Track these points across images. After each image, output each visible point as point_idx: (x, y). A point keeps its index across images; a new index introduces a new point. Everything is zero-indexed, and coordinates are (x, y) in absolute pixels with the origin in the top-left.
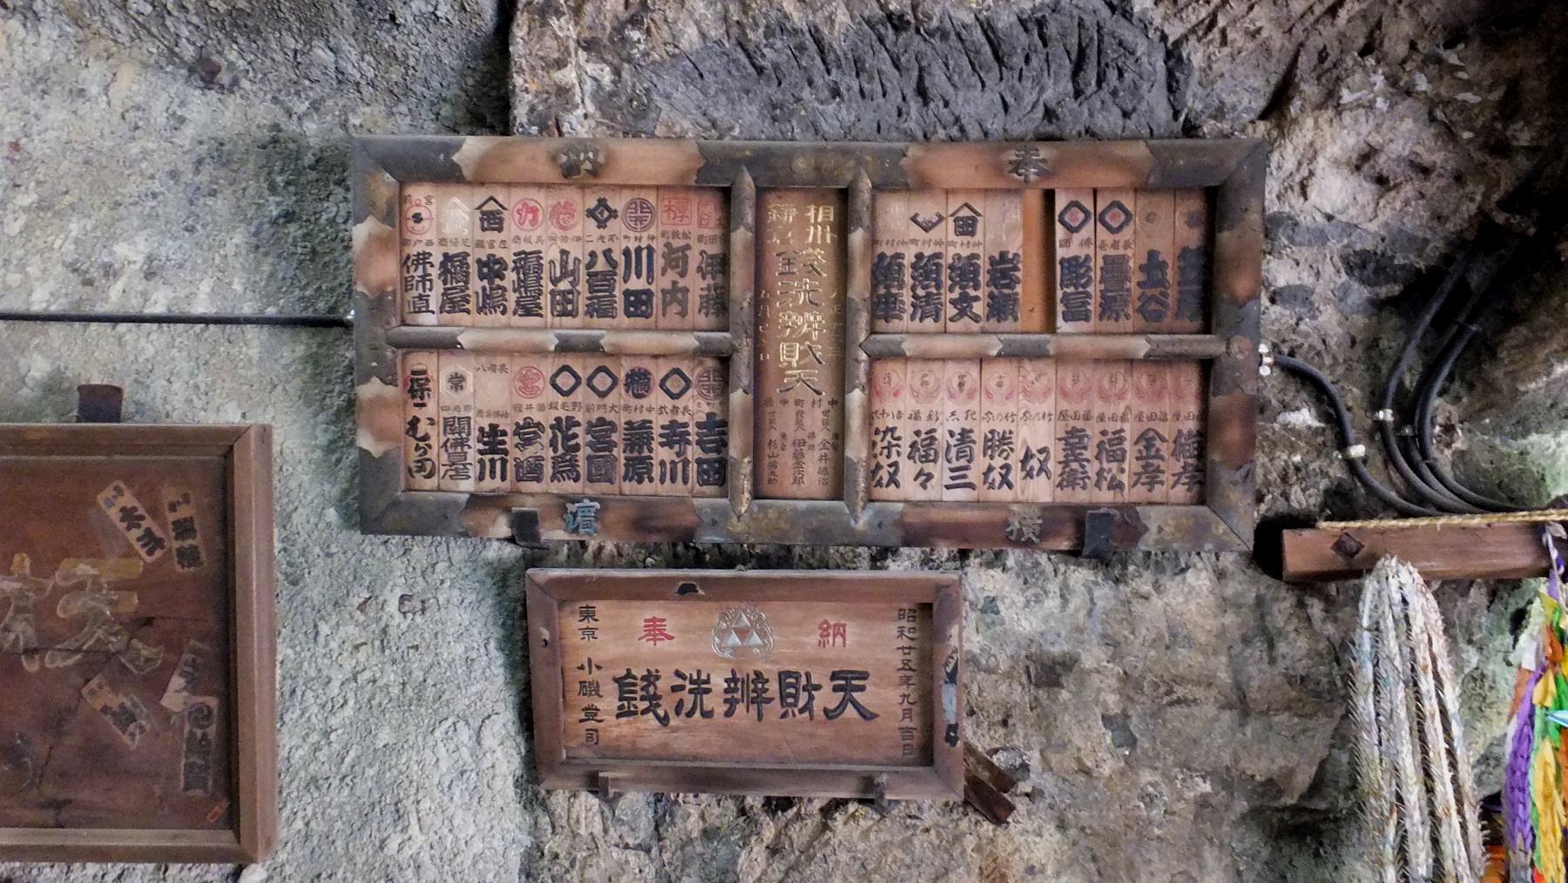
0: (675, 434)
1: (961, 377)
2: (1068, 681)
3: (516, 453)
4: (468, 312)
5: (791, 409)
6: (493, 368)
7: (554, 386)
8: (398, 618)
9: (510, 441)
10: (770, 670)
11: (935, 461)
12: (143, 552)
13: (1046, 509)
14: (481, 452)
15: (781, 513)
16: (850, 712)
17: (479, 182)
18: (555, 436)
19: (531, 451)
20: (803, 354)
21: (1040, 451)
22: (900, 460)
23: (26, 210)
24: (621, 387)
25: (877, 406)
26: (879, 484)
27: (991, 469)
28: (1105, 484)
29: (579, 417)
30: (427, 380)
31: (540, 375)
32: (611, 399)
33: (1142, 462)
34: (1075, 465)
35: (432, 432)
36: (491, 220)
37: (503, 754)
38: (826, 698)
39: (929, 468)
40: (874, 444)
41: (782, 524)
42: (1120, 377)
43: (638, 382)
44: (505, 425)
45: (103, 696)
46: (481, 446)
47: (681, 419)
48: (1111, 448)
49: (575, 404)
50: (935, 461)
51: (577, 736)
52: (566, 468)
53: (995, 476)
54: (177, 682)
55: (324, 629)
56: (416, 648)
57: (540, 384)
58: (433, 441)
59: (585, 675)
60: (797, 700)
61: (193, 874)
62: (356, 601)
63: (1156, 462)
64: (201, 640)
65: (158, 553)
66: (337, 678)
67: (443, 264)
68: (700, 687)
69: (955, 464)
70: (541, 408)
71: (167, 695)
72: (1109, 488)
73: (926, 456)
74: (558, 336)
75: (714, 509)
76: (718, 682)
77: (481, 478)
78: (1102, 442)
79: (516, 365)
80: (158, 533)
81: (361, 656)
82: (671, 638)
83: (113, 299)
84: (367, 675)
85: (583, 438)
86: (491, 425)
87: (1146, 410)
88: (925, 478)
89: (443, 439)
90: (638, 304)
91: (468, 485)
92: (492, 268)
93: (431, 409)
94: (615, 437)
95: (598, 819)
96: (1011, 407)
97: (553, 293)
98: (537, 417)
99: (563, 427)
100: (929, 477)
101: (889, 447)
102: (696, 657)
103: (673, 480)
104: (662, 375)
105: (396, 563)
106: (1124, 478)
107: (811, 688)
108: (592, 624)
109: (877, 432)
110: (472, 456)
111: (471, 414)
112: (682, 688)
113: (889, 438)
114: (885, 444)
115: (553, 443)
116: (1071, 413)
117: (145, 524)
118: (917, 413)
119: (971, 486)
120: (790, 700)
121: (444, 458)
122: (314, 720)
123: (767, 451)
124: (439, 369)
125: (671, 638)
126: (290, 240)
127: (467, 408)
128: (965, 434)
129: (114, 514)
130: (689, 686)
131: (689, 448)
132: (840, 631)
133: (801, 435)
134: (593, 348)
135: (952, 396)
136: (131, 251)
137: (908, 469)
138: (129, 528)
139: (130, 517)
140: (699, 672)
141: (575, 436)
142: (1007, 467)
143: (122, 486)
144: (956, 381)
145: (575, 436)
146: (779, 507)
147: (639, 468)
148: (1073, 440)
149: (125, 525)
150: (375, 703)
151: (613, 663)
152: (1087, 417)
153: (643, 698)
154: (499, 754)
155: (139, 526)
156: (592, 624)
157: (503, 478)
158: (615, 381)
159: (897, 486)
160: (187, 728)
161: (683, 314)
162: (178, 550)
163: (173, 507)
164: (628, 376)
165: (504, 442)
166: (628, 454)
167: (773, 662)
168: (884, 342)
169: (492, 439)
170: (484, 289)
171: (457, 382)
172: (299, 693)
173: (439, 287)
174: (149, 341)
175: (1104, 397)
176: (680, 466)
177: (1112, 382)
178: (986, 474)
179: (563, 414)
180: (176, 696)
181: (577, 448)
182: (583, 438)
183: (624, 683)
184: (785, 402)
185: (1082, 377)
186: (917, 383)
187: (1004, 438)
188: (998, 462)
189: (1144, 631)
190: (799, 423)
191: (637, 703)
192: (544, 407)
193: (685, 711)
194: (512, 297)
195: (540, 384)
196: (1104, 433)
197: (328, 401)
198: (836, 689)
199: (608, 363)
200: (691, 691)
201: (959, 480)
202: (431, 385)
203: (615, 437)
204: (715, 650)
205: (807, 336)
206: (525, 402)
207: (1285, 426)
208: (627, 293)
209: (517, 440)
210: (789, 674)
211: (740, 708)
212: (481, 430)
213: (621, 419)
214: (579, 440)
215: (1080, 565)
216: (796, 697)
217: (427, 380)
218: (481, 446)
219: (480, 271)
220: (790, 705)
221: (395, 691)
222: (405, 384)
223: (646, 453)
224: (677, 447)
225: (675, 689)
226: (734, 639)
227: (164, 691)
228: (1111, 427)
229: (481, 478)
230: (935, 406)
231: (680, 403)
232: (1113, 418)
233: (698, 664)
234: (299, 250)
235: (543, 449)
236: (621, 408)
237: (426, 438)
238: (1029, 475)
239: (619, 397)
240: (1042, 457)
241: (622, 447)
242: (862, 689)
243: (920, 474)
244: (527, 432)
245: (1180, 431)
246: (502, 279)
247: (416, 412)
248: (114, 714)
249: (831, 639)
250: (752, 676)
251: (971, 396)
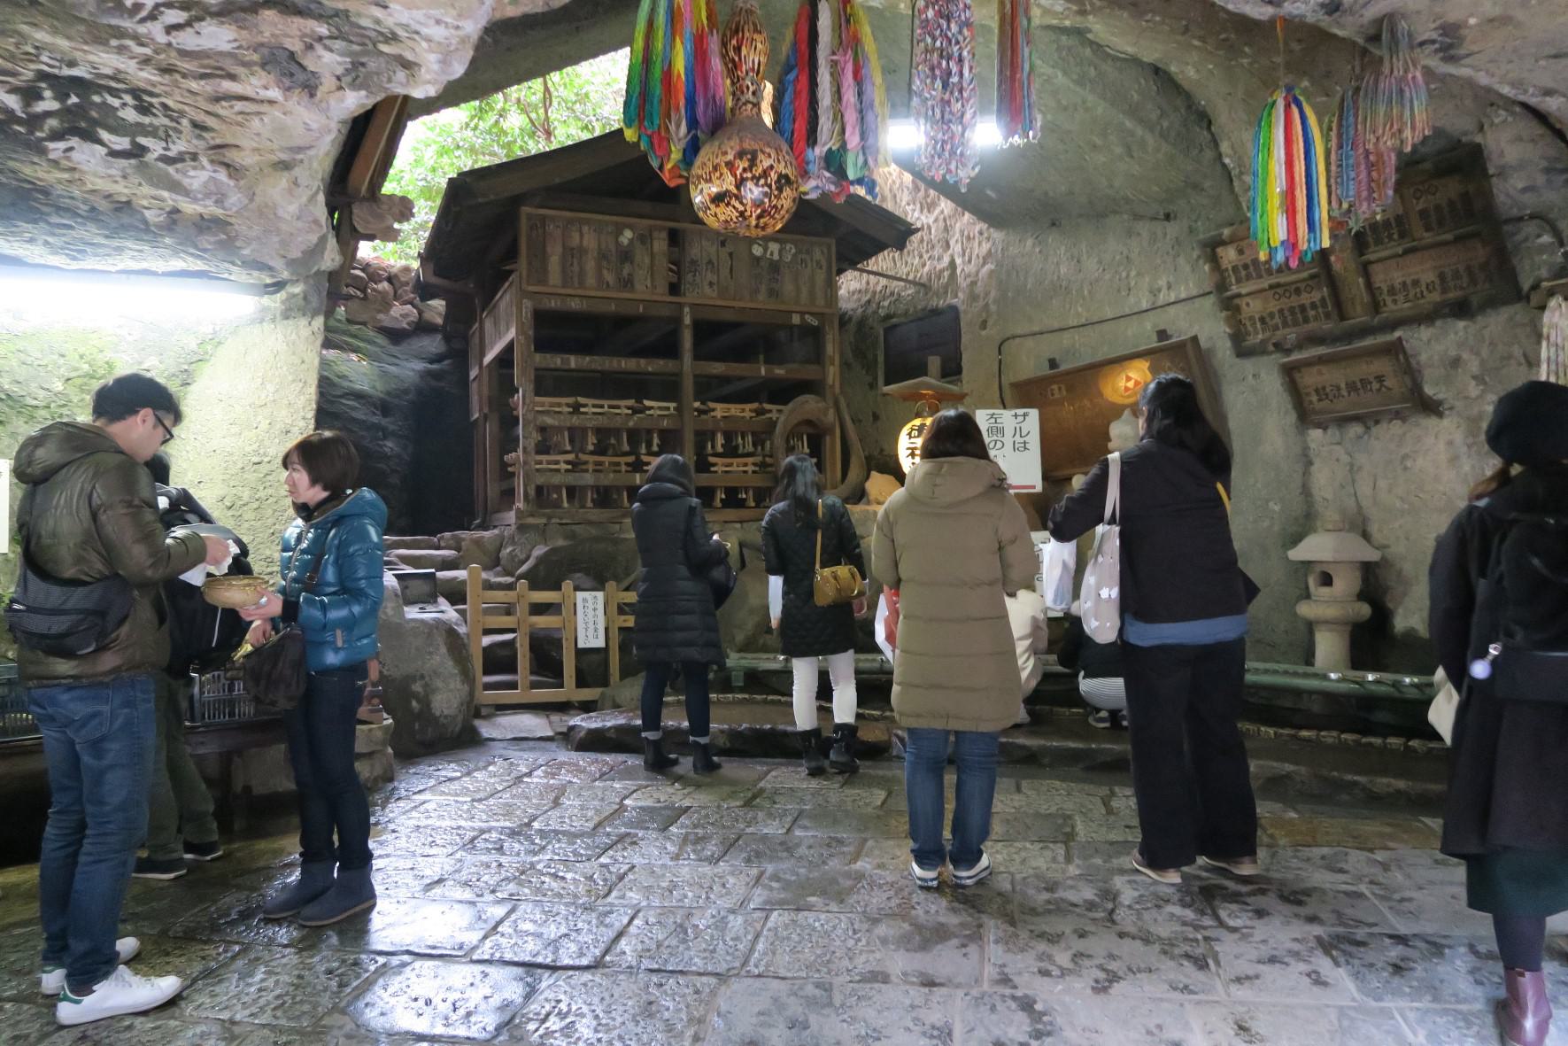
17: (1231, 242)
36: (1241, 252)
38: (1375, 386)
43: (1298, 291)
52: (1285, 324)
68: (1339, 389)
76: (1343, 386)
83: (1162, 298)
88: (1395, 302)
92: (1246, 267)
99: (1281, 311)
105: (1248, 365)
134: (1278, 285)
136: (1162, 282)
137: (1389, 300)
148: (1442, 277)
174: (1172, 310)
183: (1317, 391)
192: (1273, 306)
235: (1277, 320)
236: (1295, 301)
244: (1272, 315)
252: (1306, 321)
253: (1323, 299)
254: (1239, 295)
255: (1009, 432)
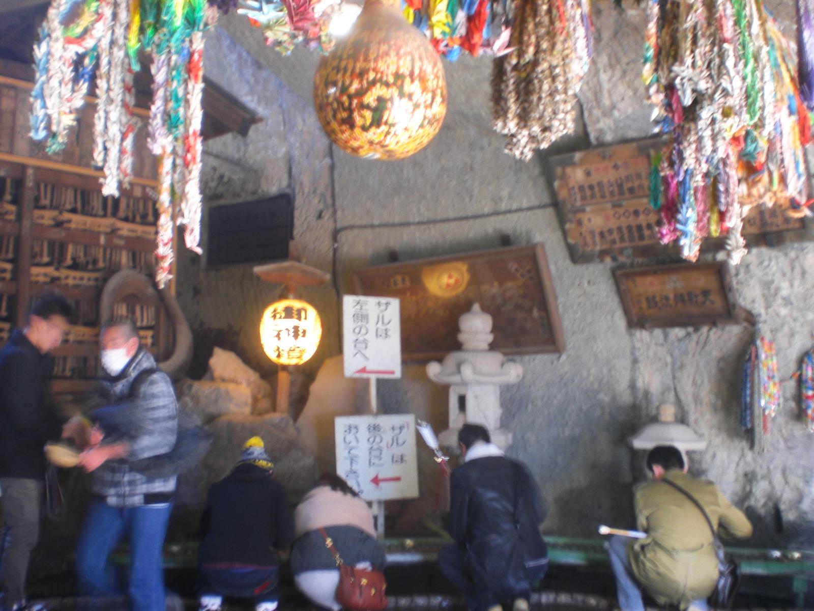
9: (607, 234)
36: (588, 174)
37: (621, 322)
38: (701, 299)
43: (636, 213)
45: (520, 315)
68: (667, 298)
83: (504, 206)
90: (631, 190)
91: (598, 248)
92: (591, 187)
99: (619, 229)
107: (696, 296)
136: (505, 193)
147: (641, 237)
169: (602, 234)
171: (589, 220)
180: (536, 313)
183: (648, 299)
235: (615, 235)
239: (632, 218)
244: (610, 231)
255: (373, 319)
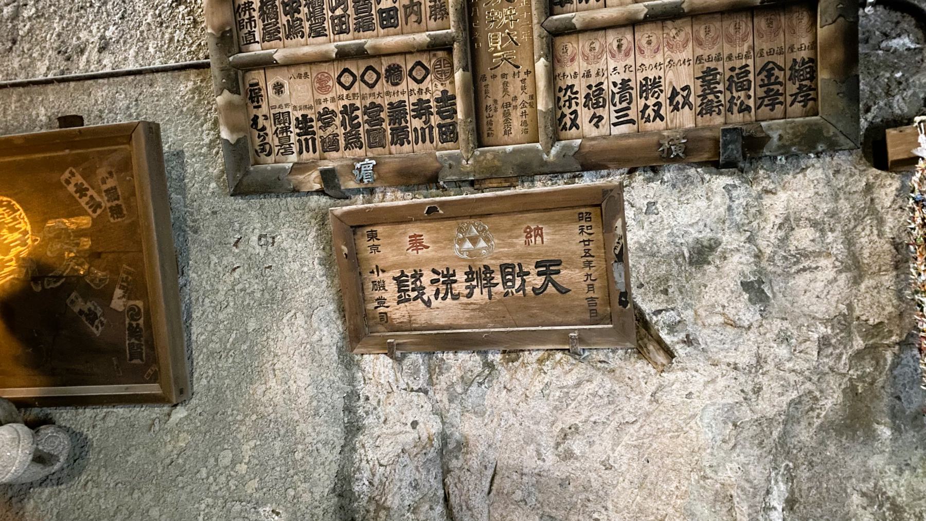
0: (422, 109)
1: (619, 41)
2: (714, 257)
3: (321, 133)
4: (280, 39)
5: (499, 81)
6: (300, 76)
7: (340, 83)
8: (258, 249)
9: (316, 125)
10: (494, 264)
11: (603, 106)
12: (90, 211)
13: (687, 133)
14: (298, 135)
15: (496, 155)
16: (551, 289)
18: (344, 118)
19: (330, 130)
20: (504, 40)
21: (683, 89)
22: (578, 108)
23: (30, 18)
24: (383, 80)
25: (559, 71)
26: (564, 128)
27: (646, 107)
28: (735, 109)
29: (358, 104)
30: (260, 89)
31: (329, 77)
32: (377, 88)
33: (765, 89)
34: (711, 97)
35: (267, 124)
37: (329, 333)
39: (600, 112)
40: (559, 99)
41: (496, 162)
42: (743, 26)
43: (394, 74)
44: (311, 114)
46: (298, 131)
47: (425, 97)
48: (739, 80)
49: (354, 94)
50: (603, 106)
51: (374, 318)
52: (353, 141)
53: (650, 111)
54: (118, 292)
55: (214, 259)
56: (270, 267)
57: (330, 83)
58: (268, 131)
59: (375, 277)
60: (514, 284)
61: (145, 413)
62: (233, 241)
63: (776, 87)
64: (129, 265)
65: (99, 211)
66: (223, 288)
67: (261, 8)
69: (619, 107)
70: (333, 100)
71: (113, 302)
72: (739, 112)
73: (598, 102)
74: (336, 47)
75: (450, 157)
77: (301, 152)
78: (731, 76)
79: (314, 71)
80: (98, 199)
81: (236, 274)
82: (428, 247)
83: (80, 67)
84: (240, 286)
85: (361, 117)
86: (302, 115)
87: (766, 47)
88: (597, 120)
89: (274, 128)
91: (293, 158)
93: (264, 109)
94: (382, 115)
95: (392, 372)
96: (659, 58)
97: (333, 18)
98: (331, 107)
99: (349, 111)
100: (601, 118)
101: (570, 99)
102: (445, 259)
103: (424, 141)
104: (409, 67)
105: (252, 214)
106: (751, 102)
107: (523, 274)
108: (376, 242)
109: (560, 90)
110: (293, 138)
111: (290, 110)
112: (438, 280)
113: (569, 93)
114: (567, 98)
115: (343, 124)
116: (705, 57)
117: (89, 193)
118: (589, 71)
119: (632, 122)
120: (509, 284)
121: (276, 142)
122: (210, 316)
123: (485, 114)
124: (265, 80)
125: (428, 247)
126: (180, 16)
127: (287, 105)
128: (625, 82)
129: (71, 188)
130: (442, 279)
131: (432, 117)
132: (539, 233)
133: (508, 99)
134: (360, 53)
135: (613, 56)
136: (90, 36)
137: (585, 115)
138: (80, 197)
139: (81, 191)
140: (448, 269)
141: (357, 117)
142: (658, 104)
143: (74, 170)
144: (615, 44)
145: (357, 117)
146: (494, 151)
148: (708, 78)
149: (78, 194)
150: (245, 303)
151: (393, 266)
152: (718, 59)
153: (413, 290)
154: (325, 332)
155: (86, 195)
156: (376, 242)
157: (314, 151)
158: (379, 75)
159: (578, 128)
160: (127, 321)
161: (419, 22)
162: (110, 208)
163: (104, 182)
164: (386, 70)
165: (312, 127)
166: (392, 126)
167: (496, 258)
168: (556, 20)
169: (304, 123)
170: (288, 21)
171: (279, 88)
172: (201, 300)
173: (260, 24)
175: (730, 40)
176: (427, 130)
177: (737, 29)
178: (643, 112)
179: (346, 102)
181: (359, 125)
182: (361, 117)
184: (494, 77)
185: (712, 29)
186: (587, 49)
187: (655, 82)
188: (652, 101)
189: (772, 218)
190: (505, 90)
191: (410, 293)
192: (335, 99)
193: (441, 295)
194: (307, 25)
195: (330, 83)
196: (733, 69)
197: (209, 116)
198: (539, 274)
199: (372, 62)
200: (443, 283)
201: (623, 118)
202: (262, 93)
203: (382, 115)
204: (457, 253)
205: (506, 26)
206: (322, 97)
207: (887, 50)
208: (381, 12)
209: (320, 124)
210: (507, 266)
211: (477, 291)
212: (297, 119)
213: (385, 102)
214: (360, 120)
215: (721, 174)
216: (513, 281)
217: (260, 89)
218: (298, 131)
219: (284, 10)
220: (510, 287)
221: (258, 295)
222: (247, 93)
223: (404, 124)
224: (424, 117)
225: (434, 282)
226: (468, 245)
227: (111, 299)
228: (738, 64)
229: (301, 152)
230: (601, 65)
231: (423, 86)
232: (739, 57)
233: (447, 264)
234: (186, 22)
235: (338, 129)
236: (386, 94)
237: (264, 128)
238: (676, 108)
239: (383, 86)
240: (685, 93)
241: (388, 121)
242: (558, 272)
243: (594, 116)
244: (326, 117)
245: (795, 60)
246: (299, 13)
247: (255, 112)
248: (86, 315)
249: (533, 239)
250: (483, 269)
251: (627, 55)
252: (400, 136)
253: (447, 100)
254: (267, 64)
